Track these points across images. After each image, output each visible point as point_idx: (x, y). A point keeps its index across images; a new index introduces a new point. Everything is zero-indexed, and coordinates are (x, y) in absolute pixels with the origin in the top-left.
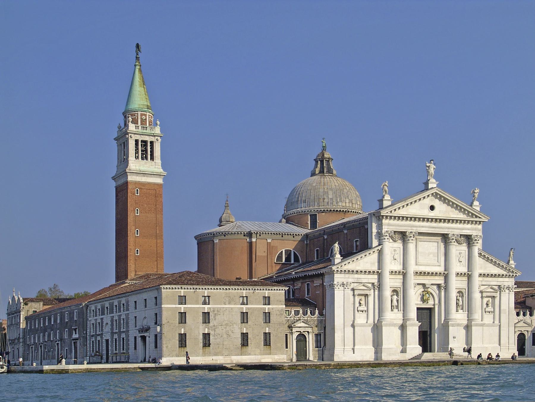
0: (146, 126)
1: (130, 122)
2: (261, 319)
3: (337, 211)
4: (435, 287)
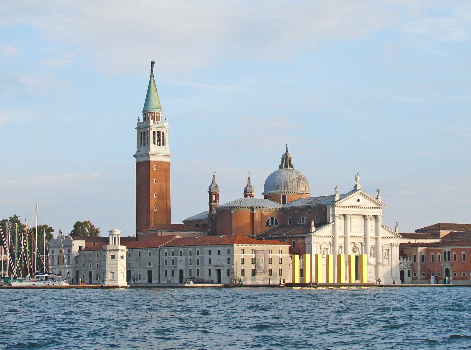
0: (159, 122)
1: (150, 120)
2: (278, 261)
3: (298, 193)
4: (360, 245)
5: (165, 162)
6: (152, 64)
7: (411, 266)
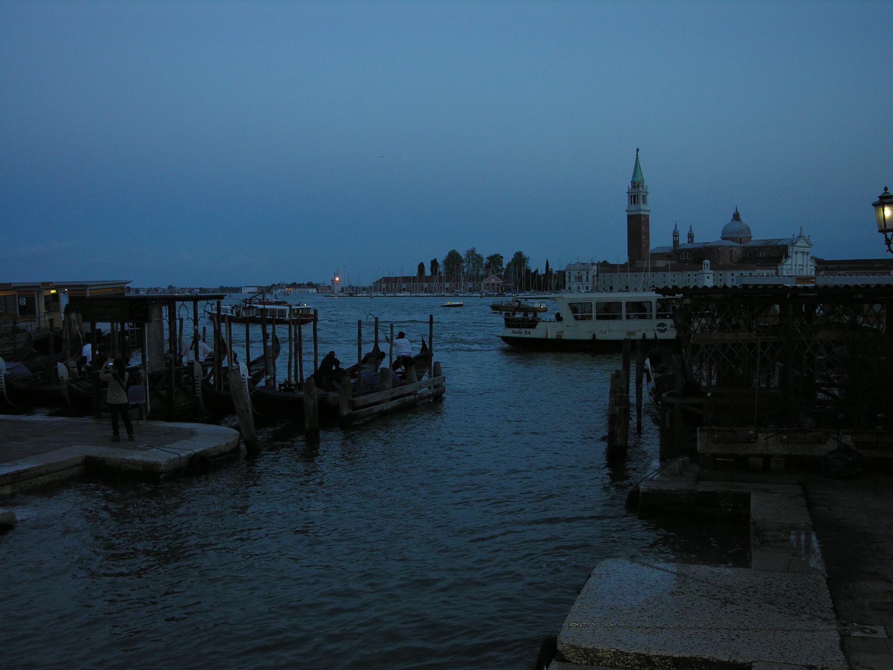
6: (638, 150)
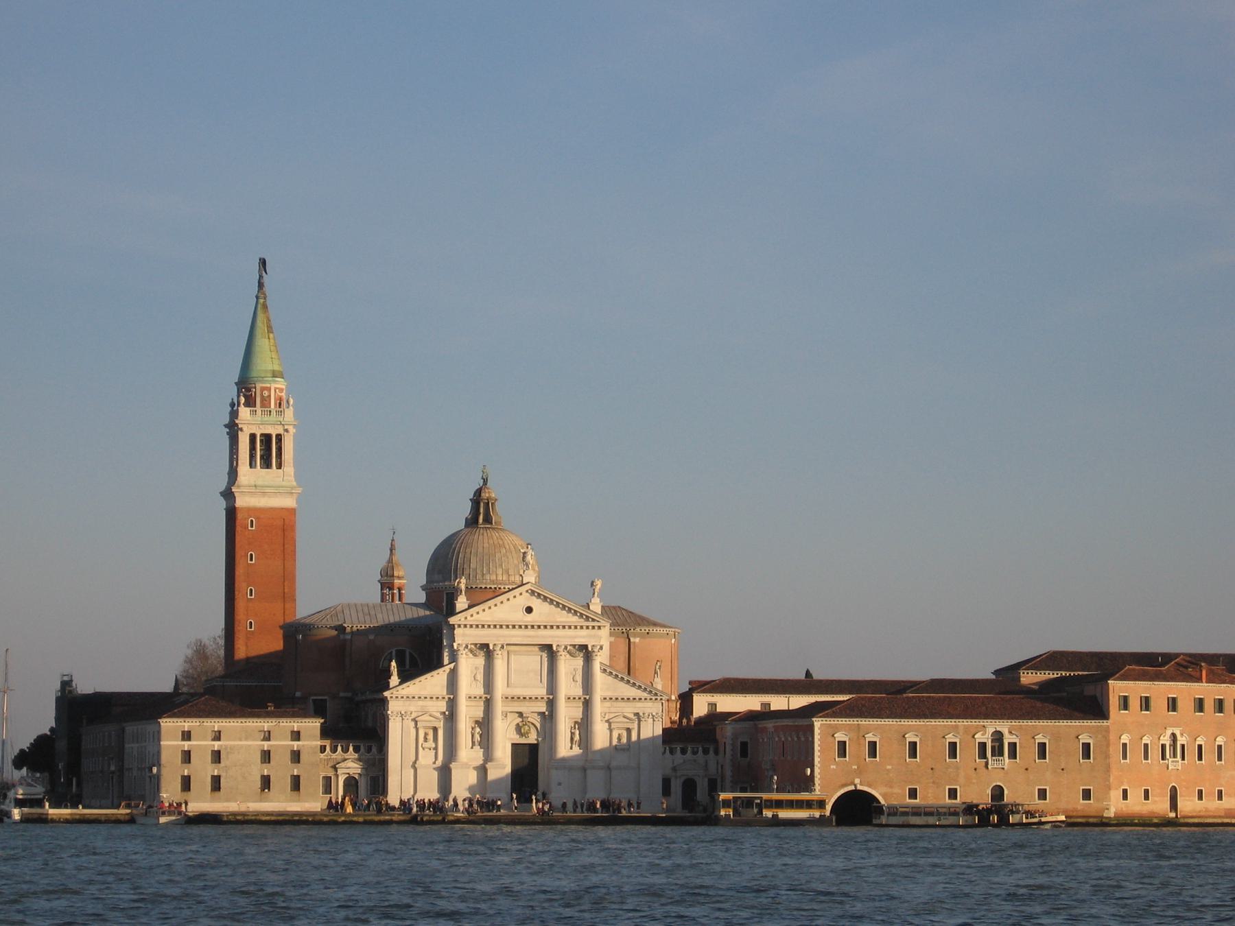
3: (481, 588)
5: (282, 509)
7: (720, 769)
